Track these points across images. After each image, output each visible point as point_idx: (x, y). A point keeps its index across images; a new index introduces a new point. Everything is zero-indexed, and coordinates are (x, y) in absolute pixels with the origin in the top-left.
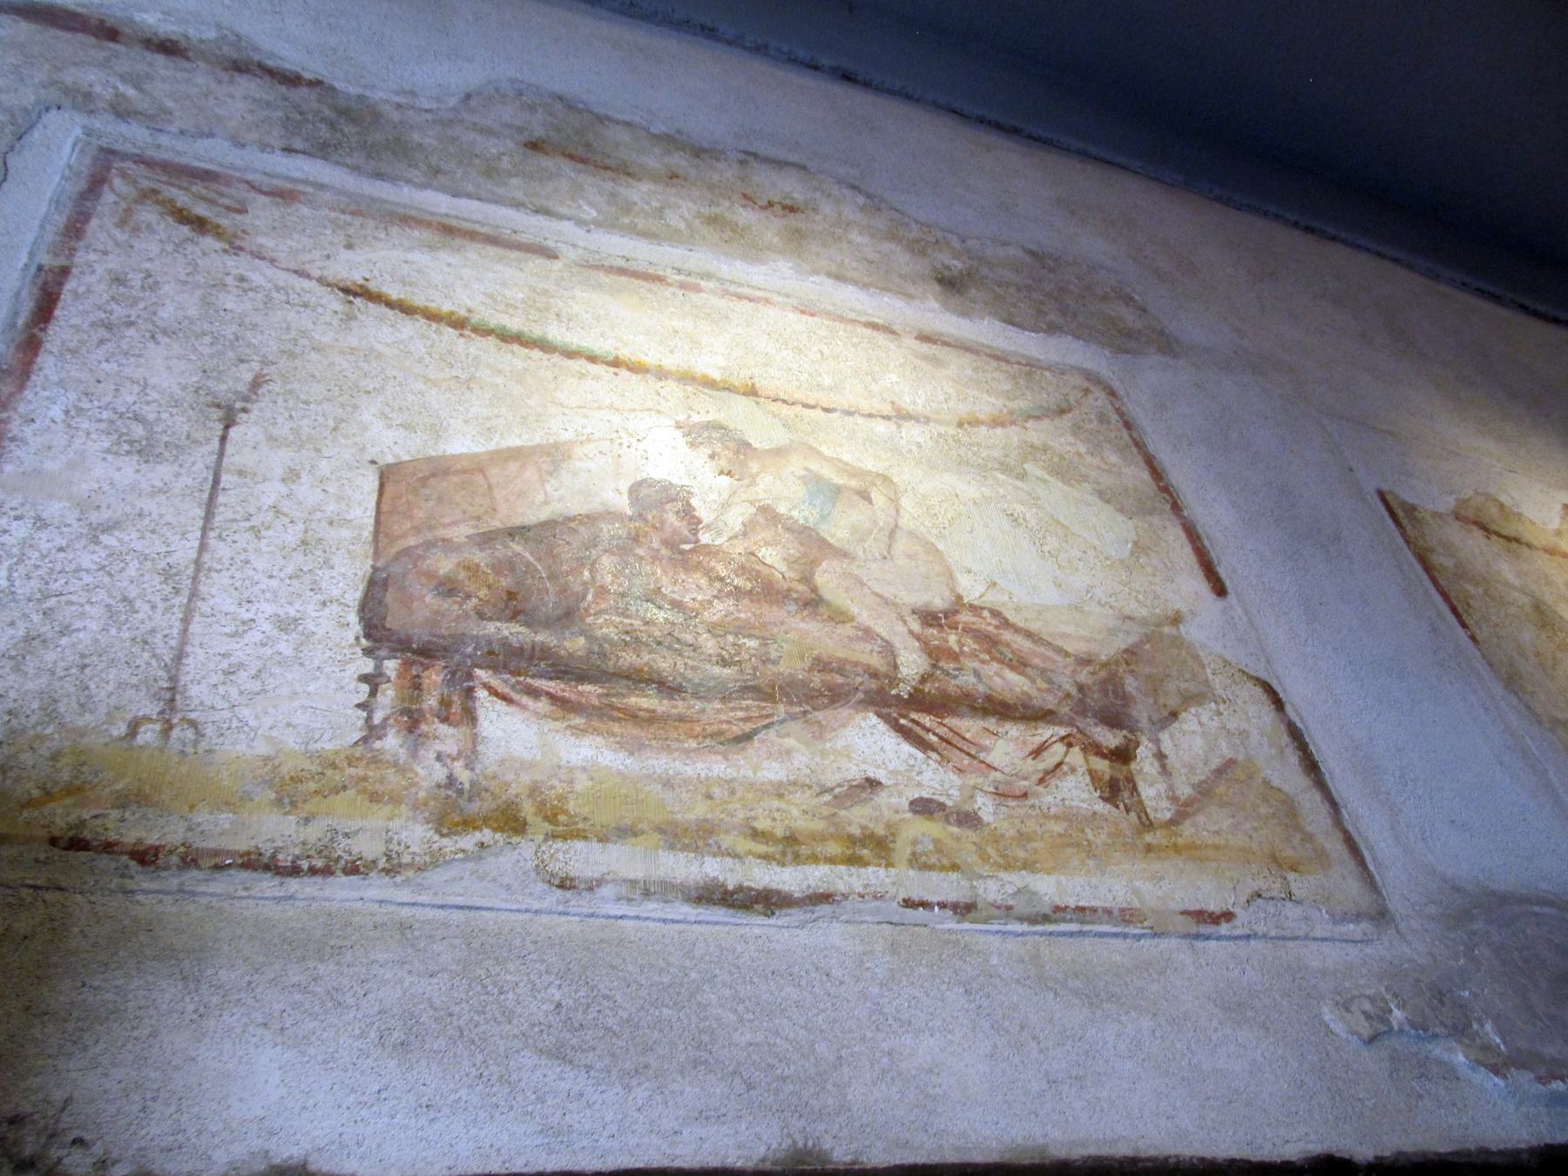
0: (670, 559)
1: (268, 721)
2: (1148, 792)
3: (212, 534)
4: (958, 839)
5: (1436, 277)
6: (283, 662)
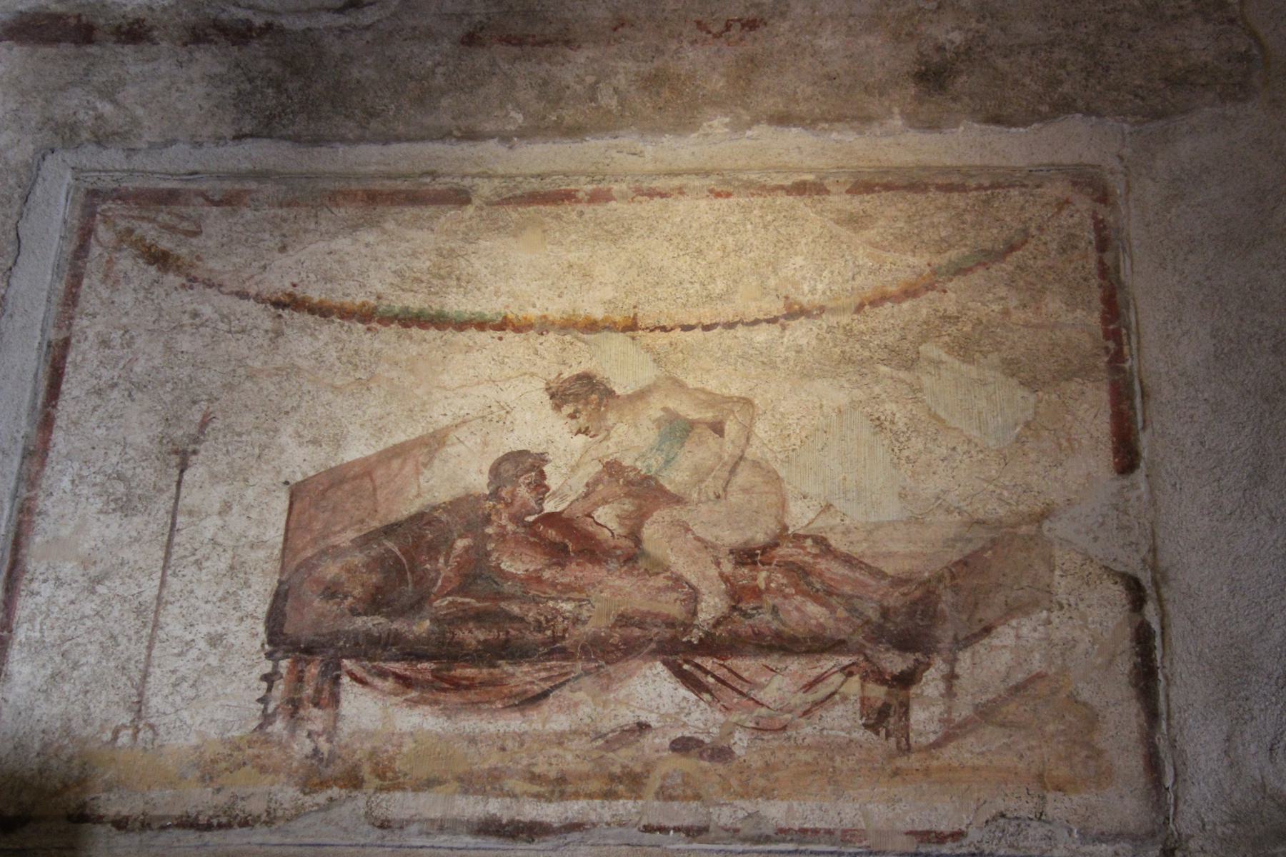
0: (514, 533)
1: (199, 719)
2: (918, 715)
3: (169, 572)
4: (705, 772)
6: (211, 671)
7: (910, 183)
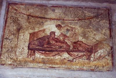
2: (91, 59)
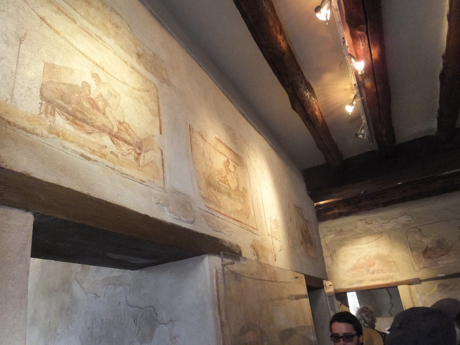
5: (217, 85)
7: (138, 72)
